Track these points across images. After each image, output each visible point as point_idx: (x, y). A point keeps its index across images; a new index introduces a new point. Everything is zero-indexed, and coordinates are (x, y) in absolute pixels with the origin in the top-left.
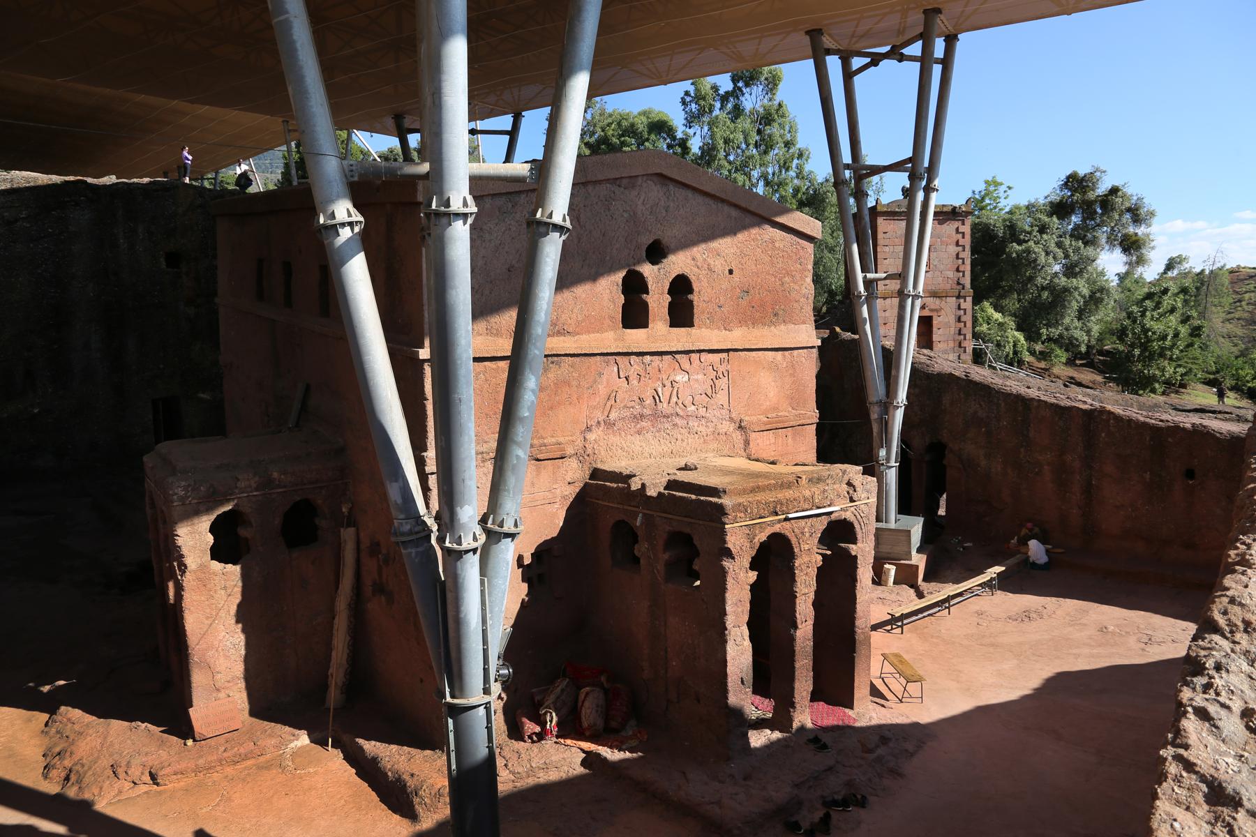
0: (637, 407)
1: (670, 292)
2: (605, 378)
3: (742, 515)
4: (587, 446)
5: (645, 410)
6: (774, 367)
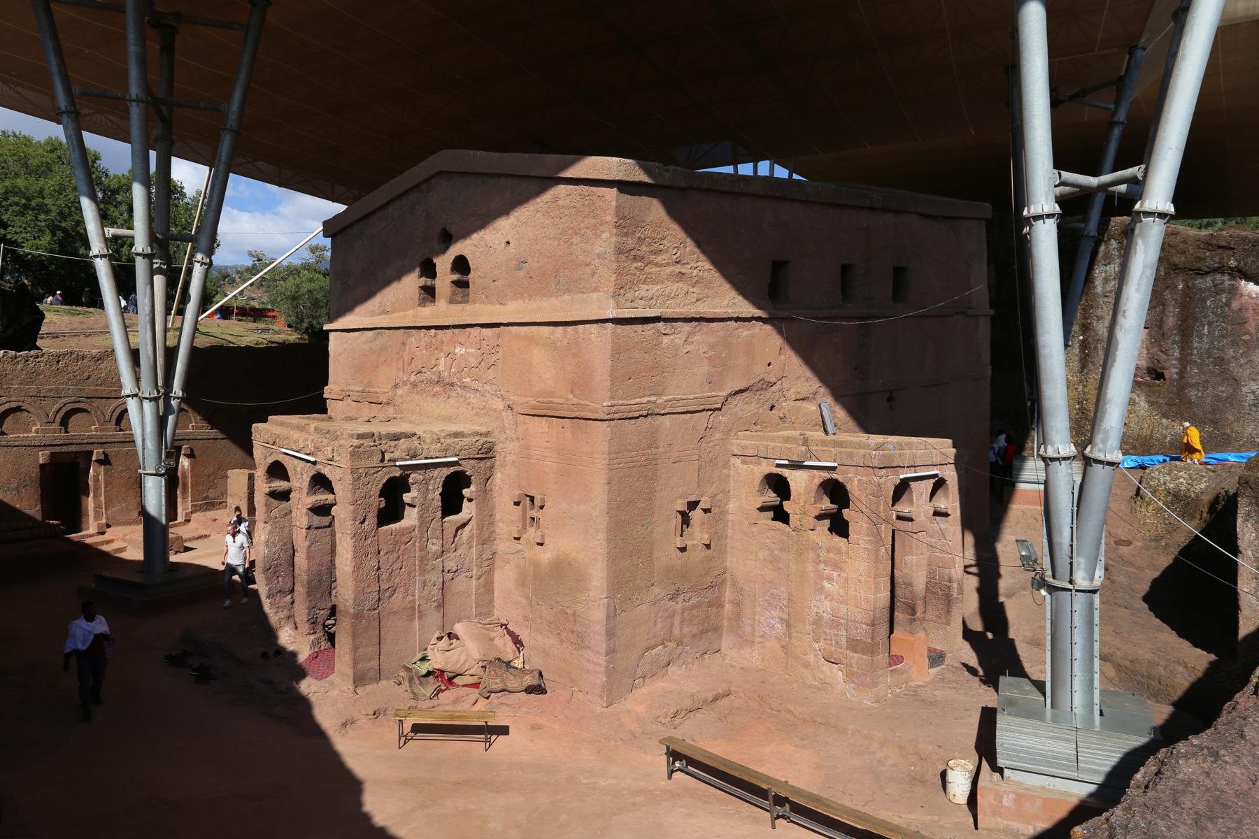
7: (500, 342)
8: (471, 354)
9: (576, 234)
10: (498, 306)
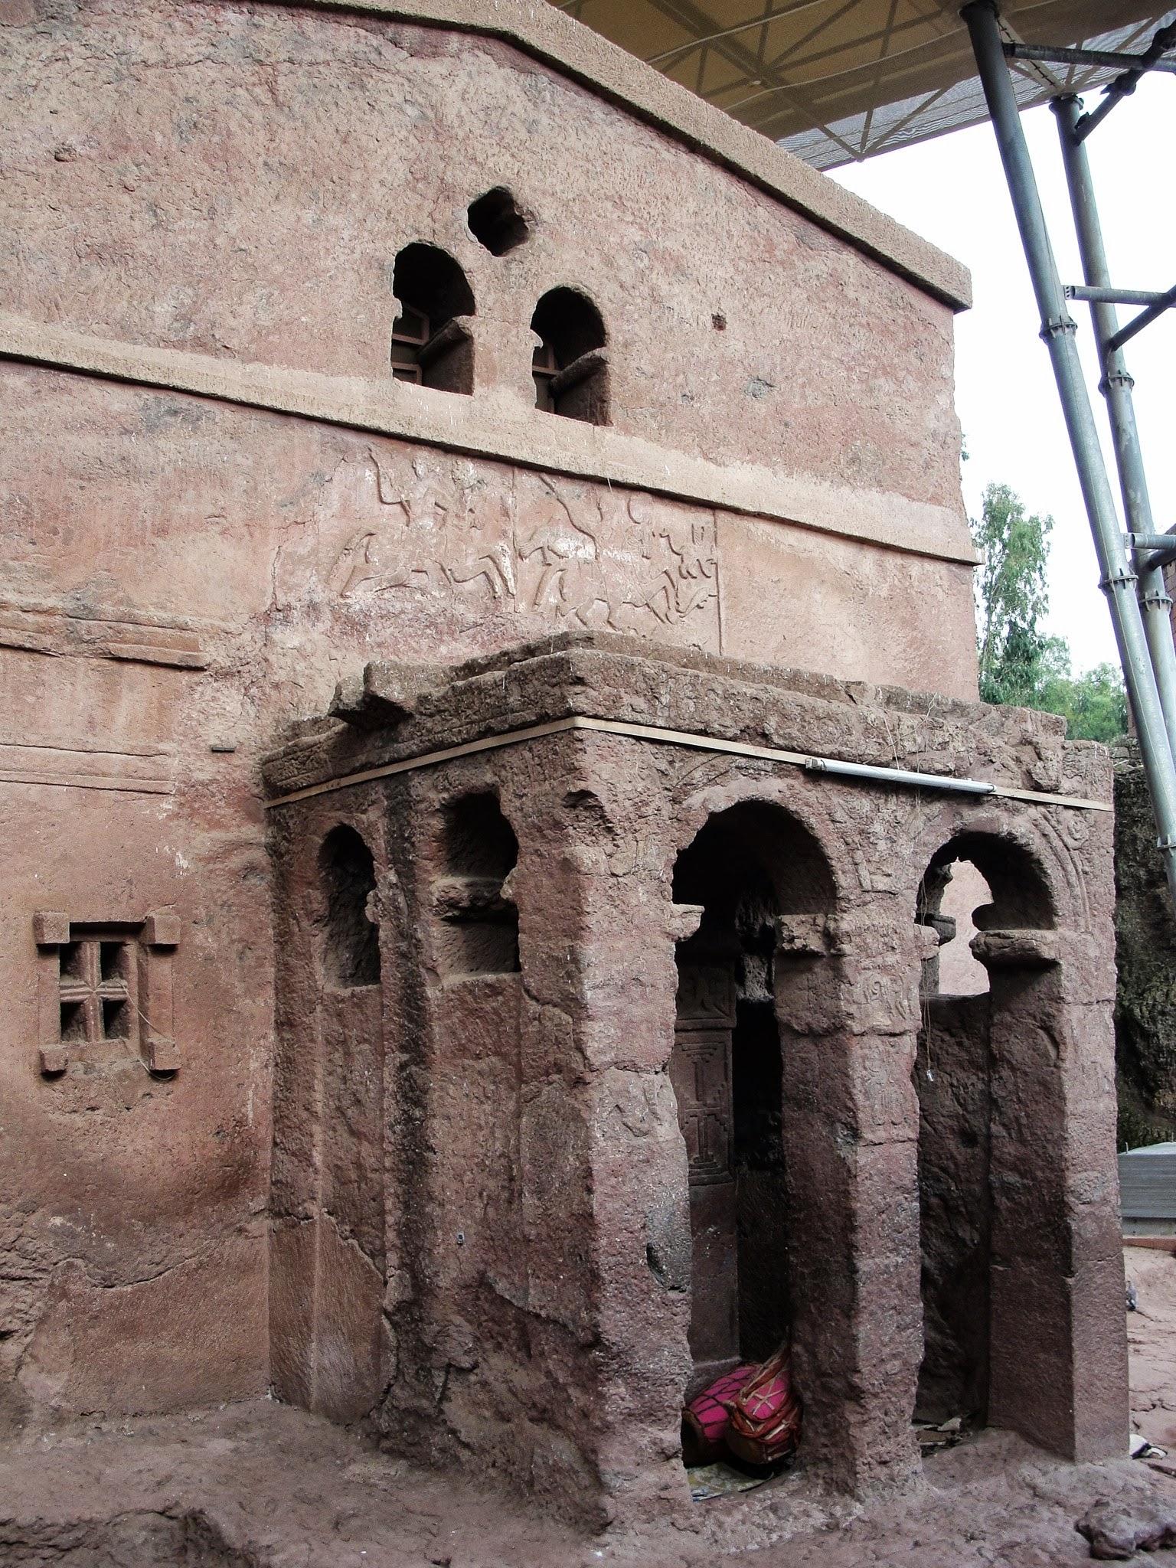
0: (435, 593)
1: (537, 324)
2: (334, 494)
3: (640, 703)
4: (272, 658)
5: (461, 608)
6: (850, 588)
7: (718, 554)
8: (621, 565)
9: (886, 374)
10: (700, 461)
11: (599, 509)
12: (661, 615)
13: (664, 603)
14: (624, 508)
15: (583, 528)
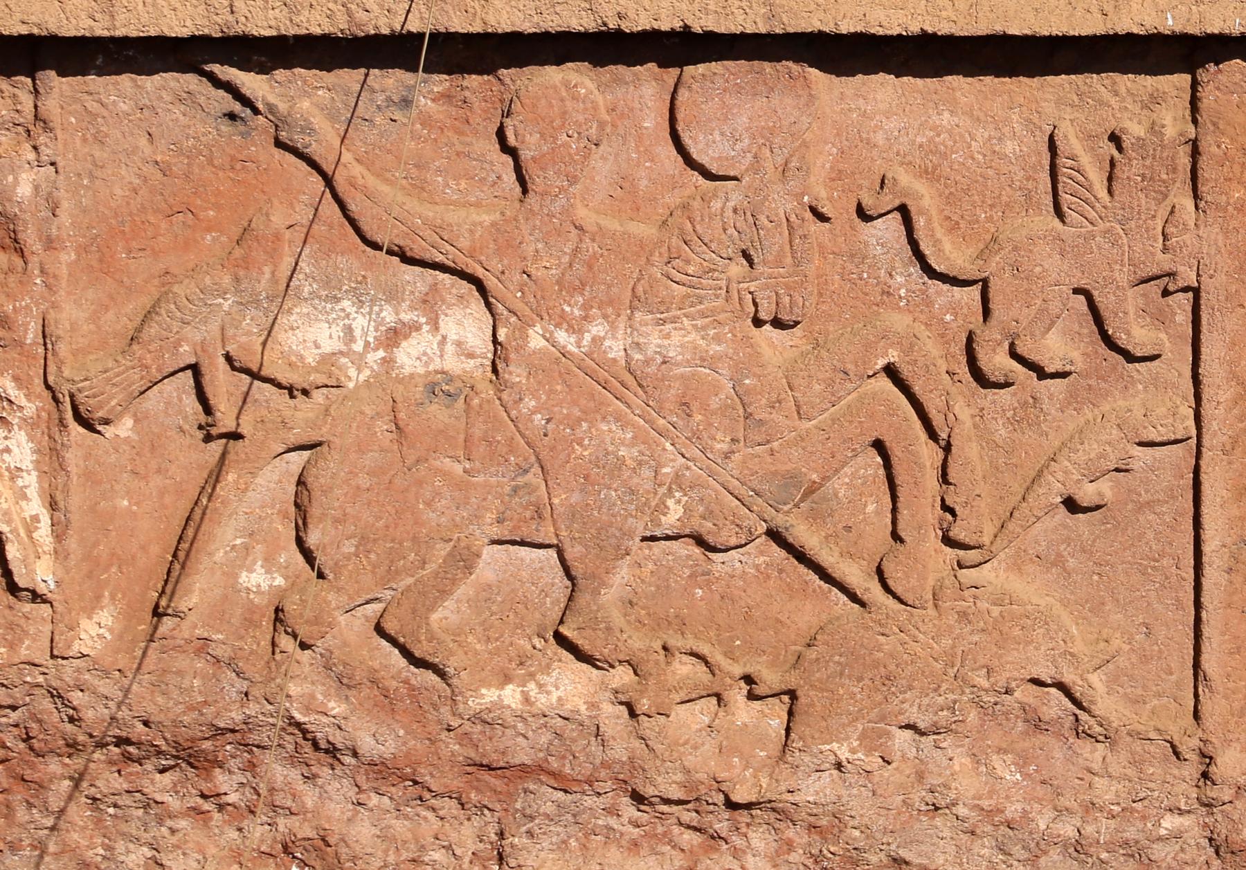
11: (506, 148)
12: (856, 575)
13: (876, 506)
14: (653, 121)
15: (418, 249)
